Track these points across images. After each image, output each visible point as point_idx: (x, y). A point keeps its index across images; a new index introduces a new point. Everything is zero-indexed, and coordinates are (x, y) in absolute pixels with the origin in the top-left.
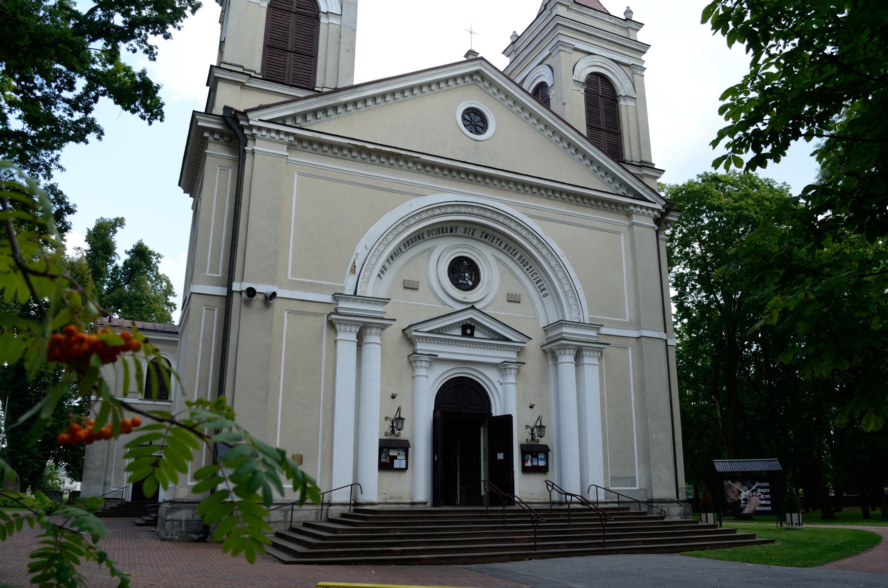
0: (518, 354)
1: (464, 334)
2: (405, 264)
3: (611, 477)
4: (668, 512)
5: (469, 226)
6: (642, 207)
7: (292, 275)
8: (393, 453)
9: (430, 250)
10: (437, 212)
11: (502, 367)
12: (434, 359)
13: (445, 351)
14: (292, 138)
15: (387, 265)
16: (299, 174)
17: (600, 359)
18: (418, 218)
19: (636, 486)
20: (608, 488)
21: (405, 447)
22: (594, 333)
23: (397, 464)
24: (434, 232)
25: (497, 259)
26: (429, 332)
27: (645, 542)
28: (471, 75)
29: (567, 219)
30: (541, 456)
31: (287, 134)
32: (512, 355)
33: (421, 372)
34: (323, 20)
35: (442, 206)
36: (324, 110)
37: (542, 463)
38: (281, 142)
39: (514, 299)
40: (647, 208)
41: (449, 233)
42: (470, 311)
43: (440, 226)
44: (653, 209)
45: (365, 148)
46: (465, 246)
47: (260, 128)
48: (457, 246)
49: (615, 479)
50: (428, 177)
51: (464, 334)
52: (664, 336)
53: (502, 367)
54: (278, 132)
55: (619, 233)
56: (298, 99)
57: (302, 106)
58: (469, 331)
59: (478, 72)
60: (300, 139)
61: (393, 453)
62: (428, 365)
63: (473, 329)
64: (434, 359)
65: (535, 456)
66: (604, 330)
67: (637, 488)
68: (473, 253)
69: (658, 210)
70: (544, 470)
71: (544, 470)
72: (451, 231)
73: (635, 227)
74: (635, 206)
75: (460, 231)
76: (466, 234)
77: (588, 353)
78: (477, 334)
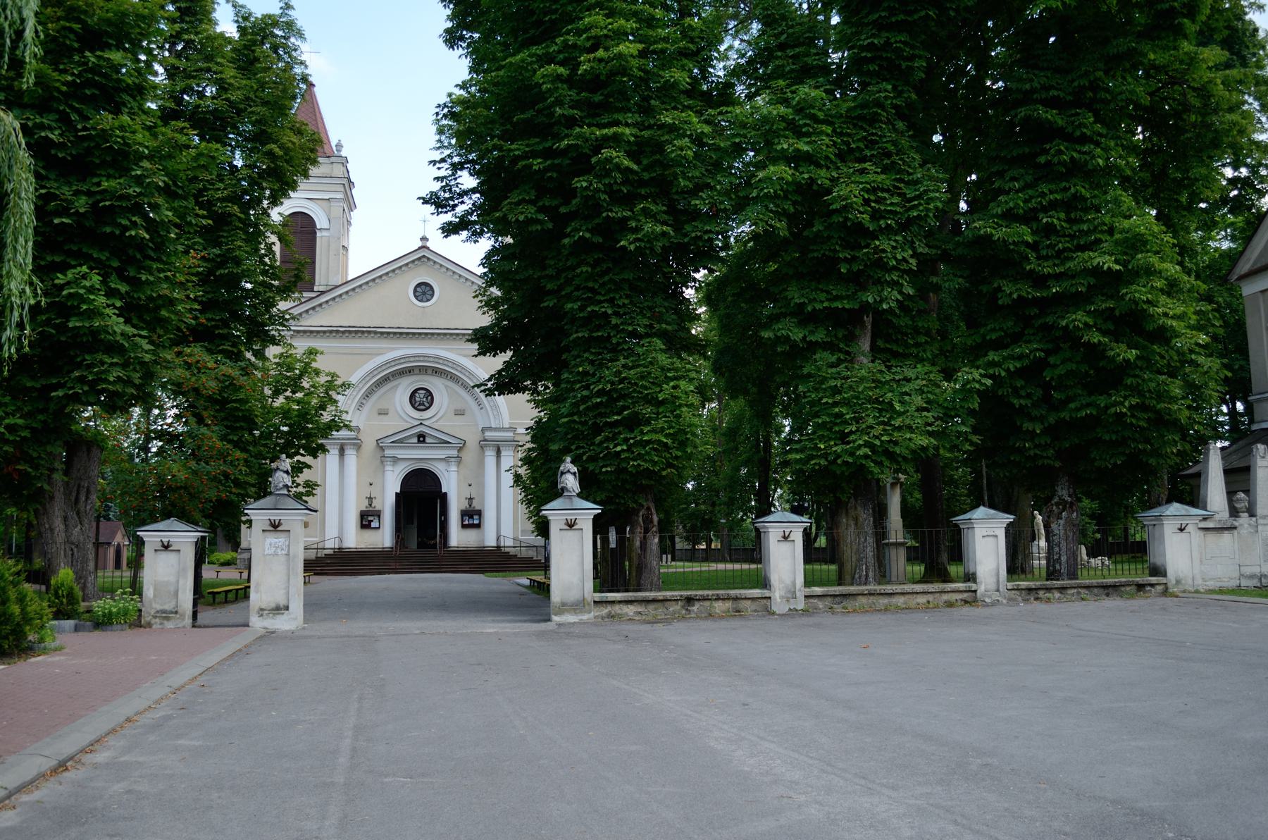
0: (459, 451)
1: (419, 441)
2: (380, 398)
8: (370, 518)
9: (397, 386)
11: (447, 460)
13: (401, 453)
15: (364, 401)
21: (378, 514)
22: (511, 434)
23: (373, 525)
25: (446, 386)
28: (419, 259)
30: (475, 517)
33: (389, 468)
34: (319, 234)
37: (476, 522)
39: (459, 413)
48: (412, 383)
49: (523, 532)
50: (386, 341)
51: (419, 441)
53: (447, 460)
59: (424, 256)
60: (298, 332)
61: (370, 518)
63: (424, 437)
64: (395, 460)
65: (471, 517)
70: (478, 526)
71: (478, 526)
75: (416, 371)
78: (428, 440)
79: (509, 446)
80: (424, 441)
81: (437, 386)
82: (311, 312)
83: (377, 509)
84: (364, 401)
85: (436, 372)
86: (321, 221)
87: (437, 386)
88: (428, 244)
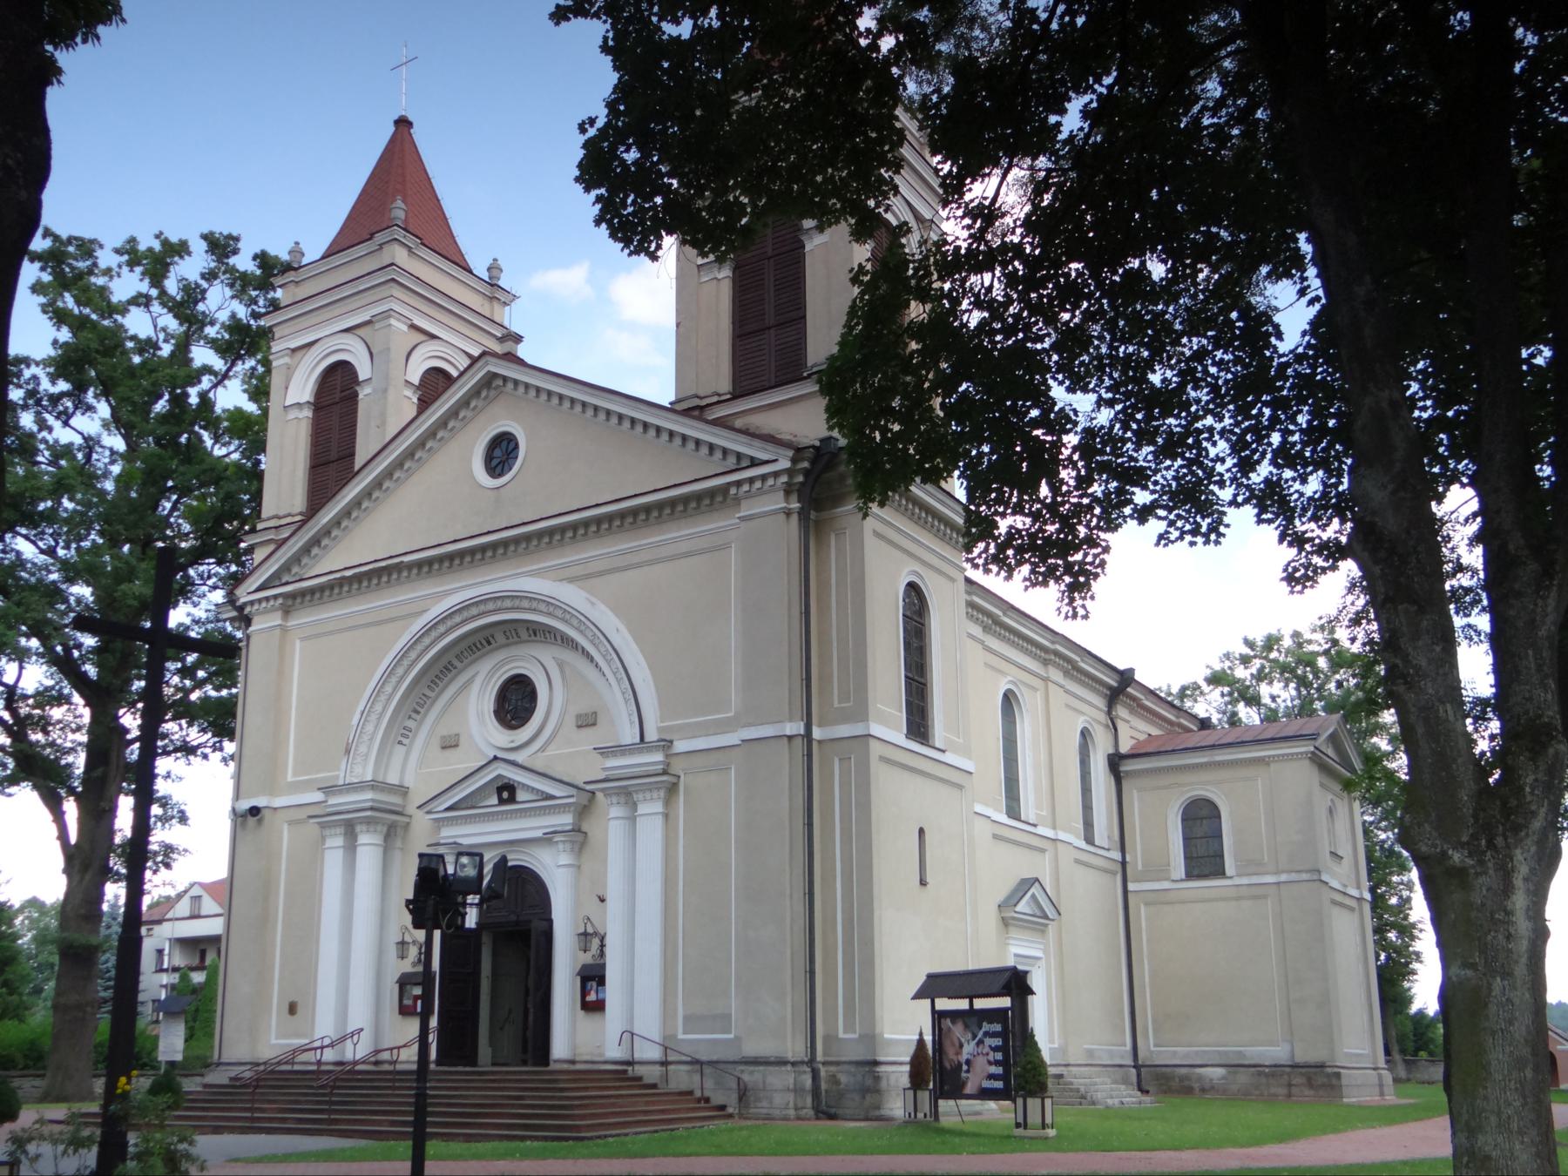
1: (502, 801)
3: (686, 1019)
4: (764, 1082)
6: (751, 480)
7: (295, 774)
10: (442, 629)
14: (280, 601)
16: (303, 639)
17: (668, 802)
18: (419, 647)
19: (684, 1033)
20: (674, 1036)
22: (658, 757)
24: (466, 654)
25: (561, 665)
27: (393, 1123)
29: (635, 559)
31: (275, 597)
32: (566, 820)
35: (445, 618)
38: (273, 609)
40: (764, 478)
41: (488, 648)
42: (496, 764)
43: (471, 640)
44: (776, 474)
45: (344, 578)
47: (252, 603)
49: (691, 1022)
51: (502, 801)
52: (795, 728)
56: (285, 540)
66: (680, 746)
67: (732, 1036)
68: (507, 667)
69: (790, 472)
72: (489, 643)
74: (738, 484)
77: (641, 796)
78: (521, 795)
79: (650, 788)
81: (533, 662)
84: (411, 724)
85: (538, 633)
87: (533, 662)
88: (522, 351)
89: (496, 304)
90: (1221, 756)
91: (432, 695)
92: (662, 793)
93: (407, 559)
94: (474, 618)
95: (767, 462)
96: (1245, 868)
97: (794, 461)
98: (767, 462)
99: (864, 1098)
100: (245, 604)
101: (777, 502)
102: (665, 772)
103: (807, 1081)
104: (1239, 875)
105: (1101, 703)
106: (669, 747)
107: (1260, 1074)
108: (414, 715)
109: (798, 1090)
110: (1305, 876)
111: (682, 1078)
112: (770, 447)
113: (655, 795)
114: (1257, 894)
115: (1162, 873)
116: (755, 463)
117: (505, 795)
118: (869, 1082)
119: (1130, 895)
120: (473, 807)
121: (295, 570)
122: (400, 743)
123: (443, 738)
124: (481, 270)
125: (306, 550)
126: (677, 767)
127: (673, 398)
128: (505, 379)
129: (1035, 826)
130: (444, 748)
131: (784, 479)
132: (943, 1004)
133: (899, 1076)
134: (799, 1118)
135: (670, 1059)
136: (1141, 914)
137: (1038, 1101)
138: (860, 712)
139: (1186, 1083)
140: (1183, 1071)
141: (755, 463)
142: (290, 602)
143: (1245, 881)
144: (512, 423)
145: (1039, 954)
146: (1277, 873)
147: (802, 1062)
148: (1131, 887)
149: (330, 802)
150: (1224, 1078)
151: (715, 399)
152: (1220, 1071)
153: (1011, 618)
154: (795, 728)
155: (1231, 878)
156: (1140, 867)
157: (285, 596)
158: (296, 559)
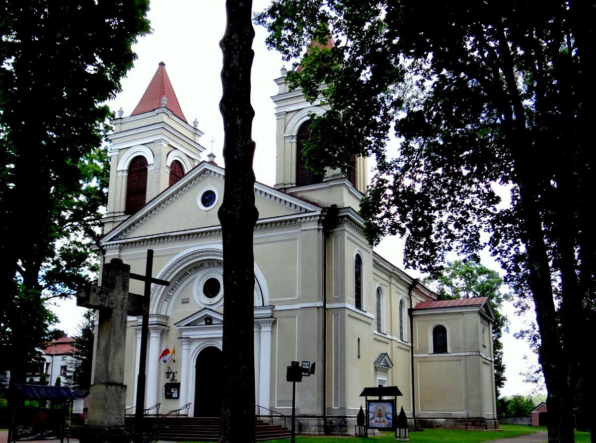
3: (278, 401)
4: (308, 423)
5: (209, 261)
6: (306, 217)
9: (194, 279)
10: (185, 260)
12: (190, 341)
13: (193, 334)
14: (119, 245)
15: (170, 294)
17: (272, 327)
20: (274, 407)
21: (177, 386)
22: (269, 311)
23: (175, 395)
26: (185, 326)
31: (116, 244)
35: (187, 256)
36: (133, 224)
40: (311, 217)
43: (195, 265)
44: (315, 216)
45: (146, 239)
46: (211, 272)
47: (107, 245)
48: (203, 276)
49: (280, 402)
51: (207, 324)
52: (321, 304)
54: (113, 244)
55: (296, 239)
57: (118, 230)
58: (208, 321)
60: (124, 244)
62: (187, 343)
64: (190, 341)
66: (277, 308)
69: (320, 216)
72: (202, 266)
73: (303, 233)
74: (301, 218)
76: (210, 266)
77: (263, 325)
80: (211, 323)
82: (132, 228)
83: (178, 382)
84: (170, 294)
86: (150, 160)
89: (196, 136)
90: (447, 311)
91: (179, 283)
92: (271, 324)
93: (172, 234)
94: (197, 257)
95: (312, 212)
96: (454, 350)
97: (322, 212)
98: (312, 212)
99: (341, 429)
100: (103, 246)
101: (315, 226)
102: (272, 317)
103: (322, 422)
104: (452, 352)
105: (407, 291)
106: (273, 308)
107: (457, 421)
108: (171, 291)
109: (319, 426)
110: (474, 353)
111: (277, 421)
112: (314, 206)
113: (268, 324)
114: (458, 359)
115: (426, 351)
116: (307, 211)
117: (208, 321)
118: (343, 423)
119: (414, 359)
120: (195, 325)
121: (124, 234)
122: (166, 300)
123: (183, 299)
124: (191, 123)
125: (129, 227)
126: (276, 315)
127: (275, 184)
128: (211, 171)
129: (386, 335)
130: (183, 303)
131: (318, 218)
132: (369, 398)
133: (353, 421)
134: (320, 435)
135: (273, 415)
136: (418, 365)
137: (404, 429)
138: (342, 299)
139: (431, 424)
140: (431, 420)
141: (307, 211)
142: (122, 246)
143: (454, 354)
144: (214, 188)
145: (386, 379)
146: (465, 352)
147: (321, 417)
148: (414, 355)
149: (139, 321)
150: (444, 422)
151: (290, 186)
152: (443, 420)
153: (381, 262)
154: (321, 304)
155: (449, 353)
156: (418, 349)
157: (121, 244)
158: (125, 230)
